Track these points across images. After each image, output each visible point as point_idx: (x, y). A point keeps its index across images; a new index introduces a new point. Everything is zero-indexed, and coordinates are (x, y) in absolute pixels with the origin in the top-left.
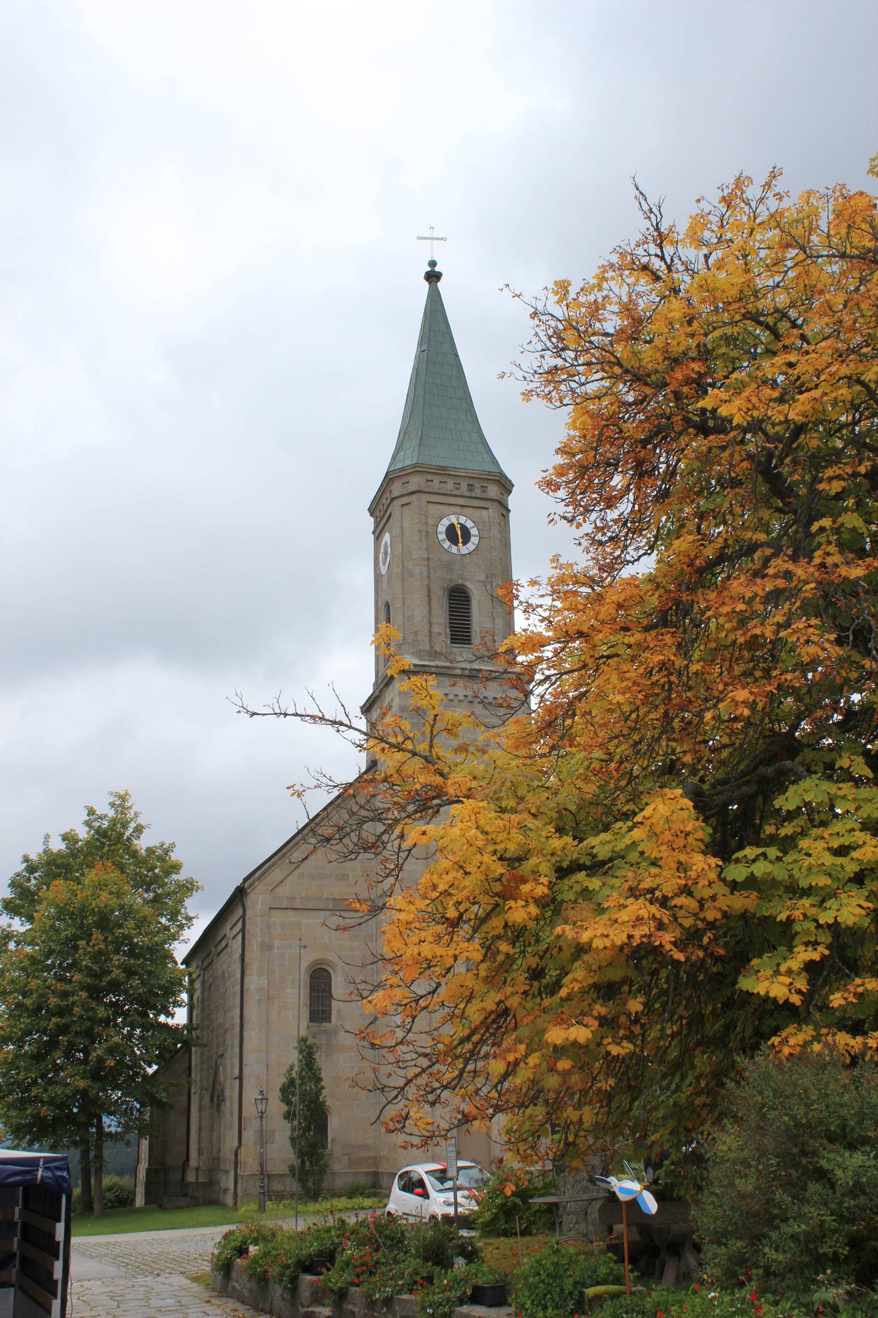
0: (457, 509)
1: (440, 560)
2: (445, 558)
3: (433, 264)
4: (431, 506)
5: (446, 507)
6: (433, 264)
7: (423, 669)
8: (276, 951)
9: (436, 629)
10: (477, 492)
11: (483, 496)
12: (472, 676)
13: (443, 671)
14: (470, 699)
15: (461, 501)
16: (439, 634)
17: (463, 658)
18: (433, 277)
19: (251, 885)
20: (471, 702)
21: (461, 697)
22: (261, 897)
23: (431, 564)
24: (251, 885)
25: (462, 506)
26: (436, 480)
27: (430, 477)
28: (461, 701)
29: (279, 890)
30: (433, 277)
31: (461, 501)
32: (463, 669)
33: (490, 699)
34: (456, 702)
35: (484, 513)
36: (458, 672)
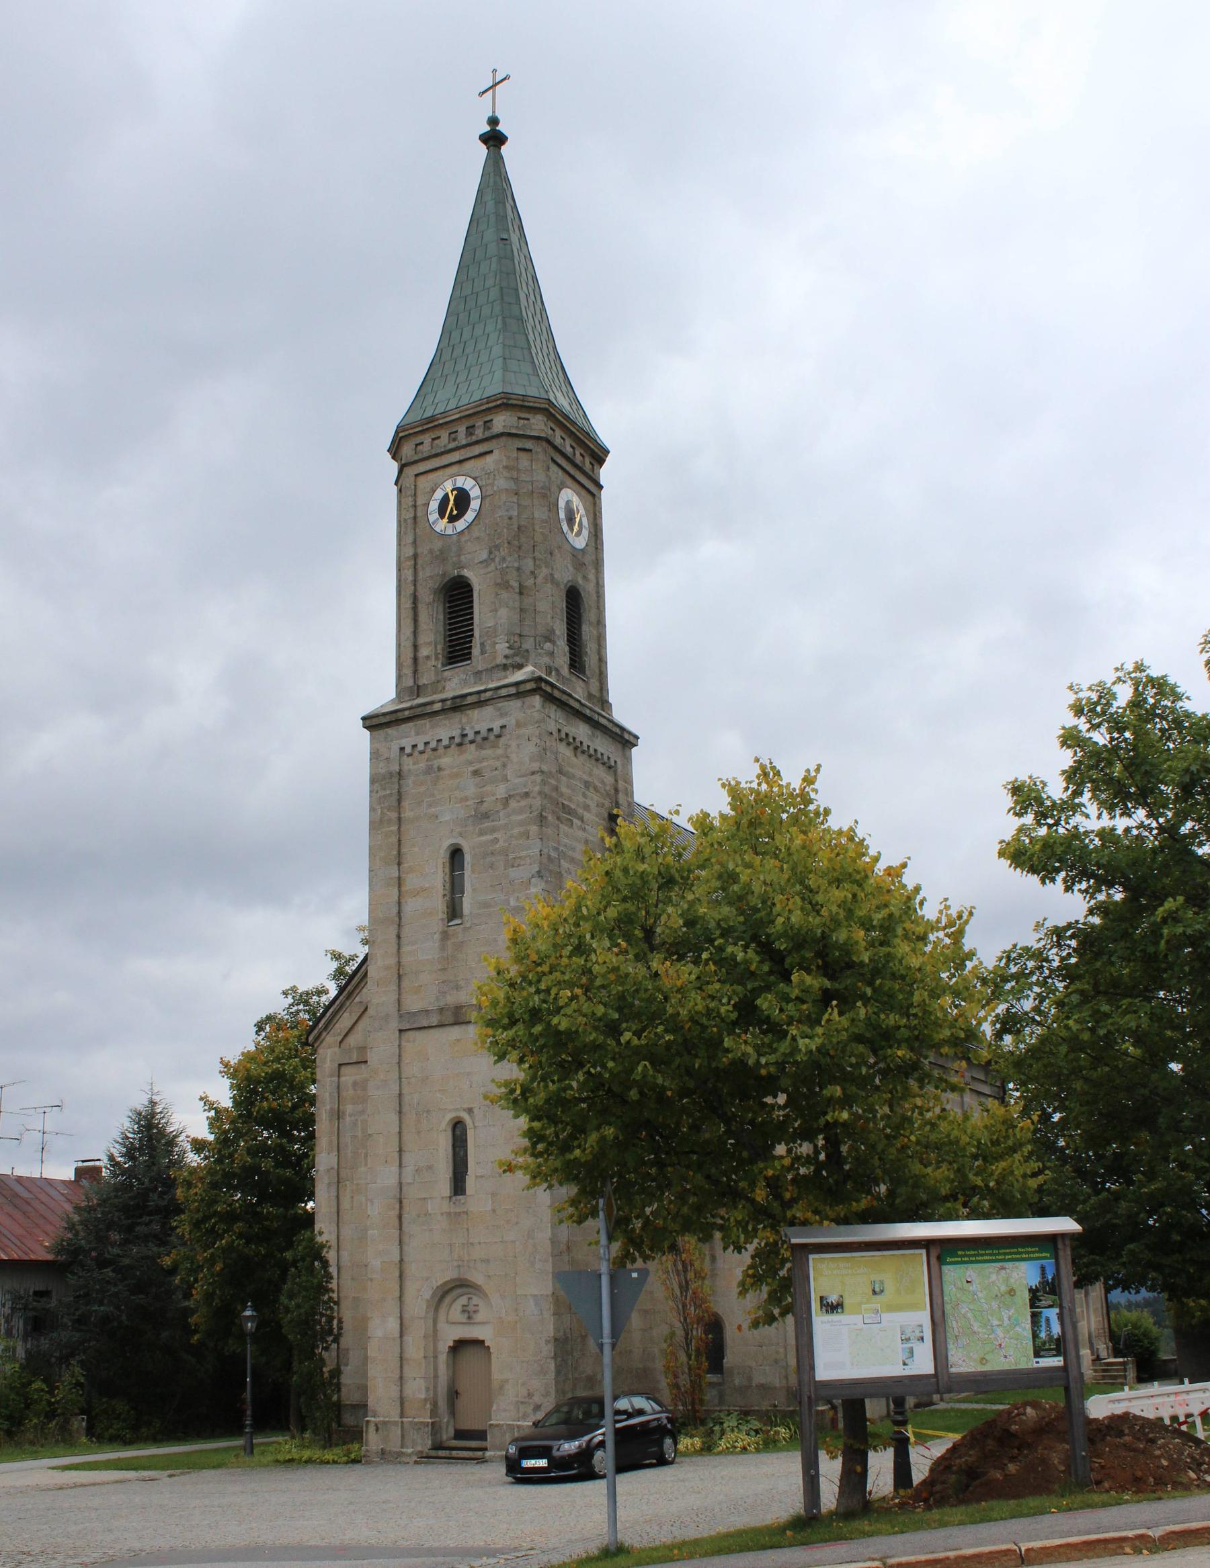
0: (454, 469)
1: (431, 551)
2: (438, 545)
3: (493, 121)
4: (421, 479)
5: (440, 473)
6: (493, 121)
7: (393, 717)
8: (348, 1119)
9: (424, 652)
10: (479, 433)
11: (487, 434)
12: (458, 705)
13: (418, 711)
14: (457, 740)
15: (456, 456)
16: (428, 658)
17: (457, 683)
18: (494, 139)
19: (317, 1039)
20: (460, 745)
21: (421, 747)
22: (329, 1052)
23: (420, 561)
24: (317, 1039)
25: (460, 462)
26: (427, 439)
27: (419, 439)
28: (446, 747)
29: (352, 1040)
30: (494, 139)
31: (456, 456)
32: (443, 701)
33: (484, 733)
34: (441, 750)
35: (489, 459)
36: (438, 707)
